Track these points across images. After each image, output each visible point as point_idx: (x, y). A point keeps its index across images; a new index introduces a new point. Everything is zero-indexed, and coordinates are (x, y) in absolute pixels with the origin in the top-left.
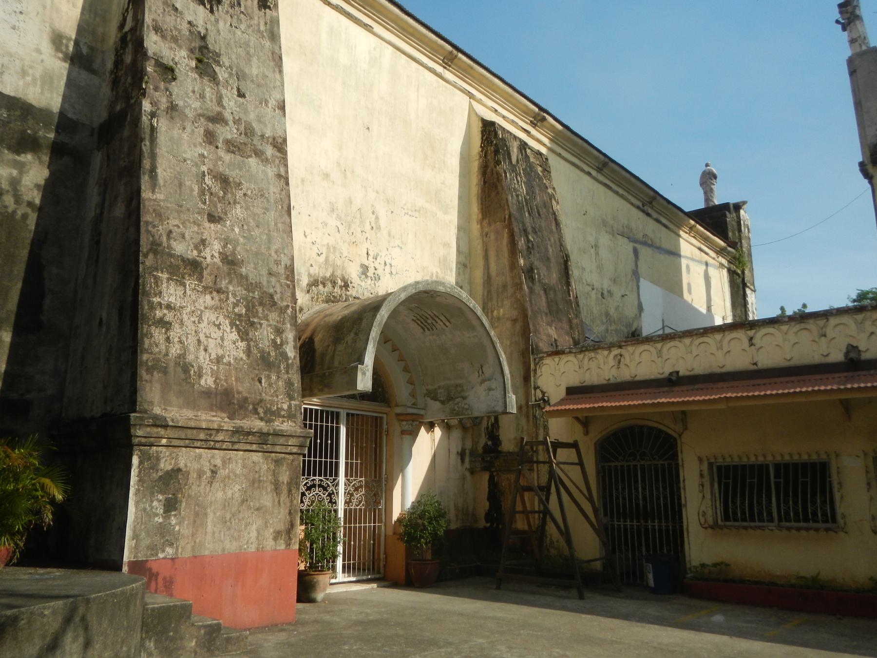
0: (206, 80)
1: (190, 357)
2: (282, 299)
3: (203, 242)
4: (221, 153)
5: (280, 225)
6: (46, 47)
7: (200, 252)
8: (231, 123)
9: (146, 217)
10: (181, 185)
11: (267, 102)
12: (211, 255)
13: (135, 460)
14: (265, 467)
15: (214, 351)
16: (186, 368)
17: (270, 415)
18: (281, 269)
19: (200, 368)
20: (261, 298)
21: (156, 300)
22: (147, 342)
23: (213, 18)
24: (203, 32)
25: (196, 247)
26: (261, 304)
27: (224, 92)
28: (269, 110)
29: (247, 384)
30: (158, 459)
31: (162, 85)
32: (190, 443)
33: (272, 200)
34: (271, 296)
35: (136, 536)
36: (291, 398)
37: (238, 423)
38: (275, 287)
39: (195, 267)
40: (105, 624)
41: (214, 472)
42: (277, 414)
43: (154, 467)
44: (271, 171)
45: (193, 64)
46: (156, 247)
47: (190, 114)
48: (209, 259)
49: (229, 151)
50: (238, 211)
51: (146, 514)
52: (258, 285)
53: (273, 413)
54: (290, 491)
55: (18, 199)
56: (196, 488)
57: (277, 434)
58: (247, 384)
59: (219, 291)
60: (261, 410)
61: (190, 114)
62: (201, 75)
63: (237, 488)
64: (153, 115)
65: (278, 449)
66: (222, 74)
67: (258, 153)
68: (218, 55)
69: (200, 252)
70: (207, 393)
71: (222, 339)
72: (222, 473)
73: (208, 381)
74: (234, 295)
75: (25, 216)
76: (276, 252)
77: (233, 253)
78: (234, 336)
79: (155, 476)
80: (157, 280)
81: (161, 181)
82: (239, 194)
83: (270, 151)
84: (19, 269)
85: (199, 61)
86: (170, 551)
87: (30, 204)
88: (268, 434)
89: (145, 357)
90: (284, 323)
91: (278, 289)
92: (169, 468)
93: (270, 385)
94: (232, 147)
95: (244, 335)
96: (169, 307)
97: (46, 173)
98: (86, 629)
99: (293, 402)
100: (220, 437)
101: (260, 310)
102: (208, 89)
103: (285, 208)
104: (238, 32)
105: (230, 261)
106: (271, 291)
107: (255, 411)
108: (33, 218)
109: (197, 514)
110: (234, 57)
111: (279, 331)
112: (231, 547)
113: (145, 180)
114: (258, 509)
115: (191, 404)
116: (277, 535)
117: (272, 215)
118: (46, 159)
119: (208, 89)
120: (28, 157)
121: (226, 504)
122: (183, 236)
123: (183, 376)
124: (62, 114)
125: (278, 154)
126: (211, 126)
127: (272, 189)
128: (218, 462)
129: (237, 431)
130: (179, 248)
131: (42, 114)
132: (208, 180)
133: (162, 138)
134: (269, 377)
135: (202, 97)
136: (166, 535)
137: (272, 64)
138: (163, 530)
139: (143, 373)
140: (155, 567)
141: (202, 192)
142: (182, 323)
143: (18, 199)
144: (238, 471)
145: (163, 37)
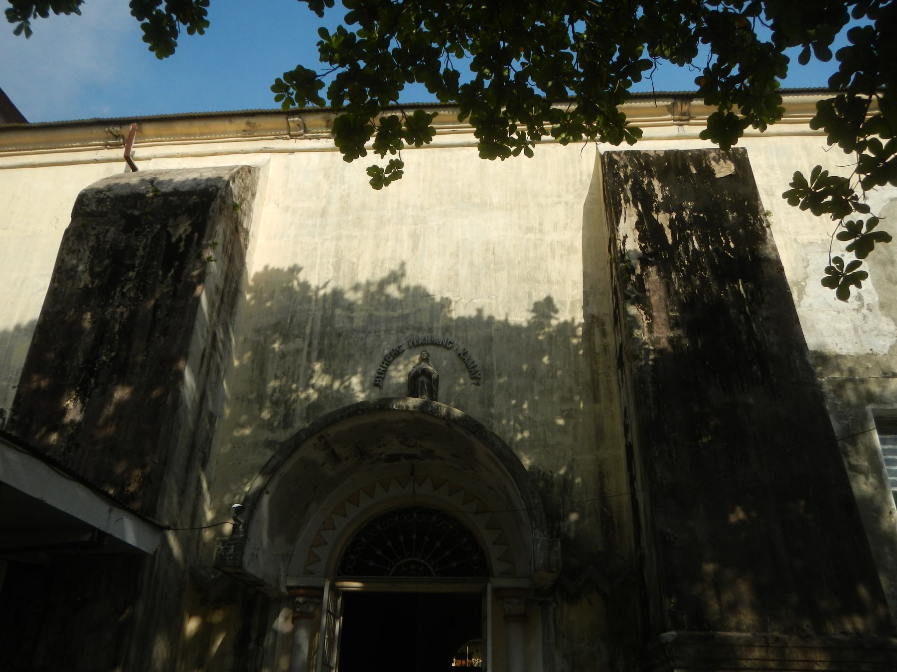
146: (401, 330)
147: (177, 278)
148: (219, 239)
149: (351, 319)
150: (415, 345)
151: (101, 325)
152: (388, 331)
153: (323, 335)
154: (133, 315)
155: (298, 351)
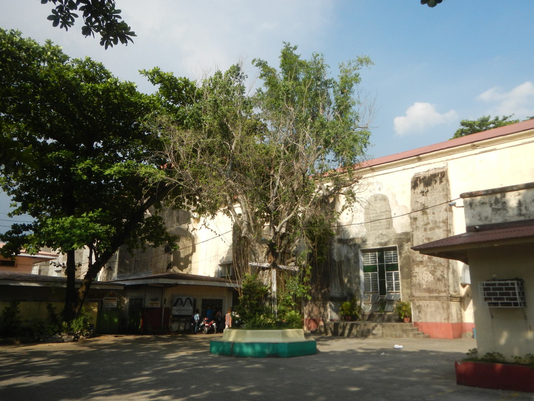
0: (424, 216)
1: (421, 282)
11: (441, 211)
16: (420, 285)
17: (440, 292)
20: (438, 264)
21: (413, 272)
23: (426, 197)
24: (423, 203)
26: (438, 266)
28: (441, 213)
32: (421, 300)
34: (441, 263)
35: (414, 317)
37: (431, 295)
41: (427, 305)
42: (441, 292)
43: (415, 304)
44: (441, 230)
49: (430, 230)
53: (440, 291)
54: (447, 309)
59: (427, 266)
60: (437, 291)
61: (421, 226)
62: (423, 215)
67: (438, 227)
70: (424, 289)
72: (429, 305)
73: (424, 287)
78: (431, 275)
79: (416, 306)
80: (414, 267)
83: (441, 225)
86: (420, 321)
94: (432, 229)
95: (433, 275)
96: (416, 273)
101: (437, 268)
104: (433, 196)
107: (436, 292)
111: (442, 272)
112: (434, 321)
116: (445, 319)
121: (431, 312)
125: (444, 224)
128: (428, 303)
129: (430, 297)
133: (415, 236)
135: (424, 220)
138: (419, 317)
140: (418, 323)
142: (419, 275)
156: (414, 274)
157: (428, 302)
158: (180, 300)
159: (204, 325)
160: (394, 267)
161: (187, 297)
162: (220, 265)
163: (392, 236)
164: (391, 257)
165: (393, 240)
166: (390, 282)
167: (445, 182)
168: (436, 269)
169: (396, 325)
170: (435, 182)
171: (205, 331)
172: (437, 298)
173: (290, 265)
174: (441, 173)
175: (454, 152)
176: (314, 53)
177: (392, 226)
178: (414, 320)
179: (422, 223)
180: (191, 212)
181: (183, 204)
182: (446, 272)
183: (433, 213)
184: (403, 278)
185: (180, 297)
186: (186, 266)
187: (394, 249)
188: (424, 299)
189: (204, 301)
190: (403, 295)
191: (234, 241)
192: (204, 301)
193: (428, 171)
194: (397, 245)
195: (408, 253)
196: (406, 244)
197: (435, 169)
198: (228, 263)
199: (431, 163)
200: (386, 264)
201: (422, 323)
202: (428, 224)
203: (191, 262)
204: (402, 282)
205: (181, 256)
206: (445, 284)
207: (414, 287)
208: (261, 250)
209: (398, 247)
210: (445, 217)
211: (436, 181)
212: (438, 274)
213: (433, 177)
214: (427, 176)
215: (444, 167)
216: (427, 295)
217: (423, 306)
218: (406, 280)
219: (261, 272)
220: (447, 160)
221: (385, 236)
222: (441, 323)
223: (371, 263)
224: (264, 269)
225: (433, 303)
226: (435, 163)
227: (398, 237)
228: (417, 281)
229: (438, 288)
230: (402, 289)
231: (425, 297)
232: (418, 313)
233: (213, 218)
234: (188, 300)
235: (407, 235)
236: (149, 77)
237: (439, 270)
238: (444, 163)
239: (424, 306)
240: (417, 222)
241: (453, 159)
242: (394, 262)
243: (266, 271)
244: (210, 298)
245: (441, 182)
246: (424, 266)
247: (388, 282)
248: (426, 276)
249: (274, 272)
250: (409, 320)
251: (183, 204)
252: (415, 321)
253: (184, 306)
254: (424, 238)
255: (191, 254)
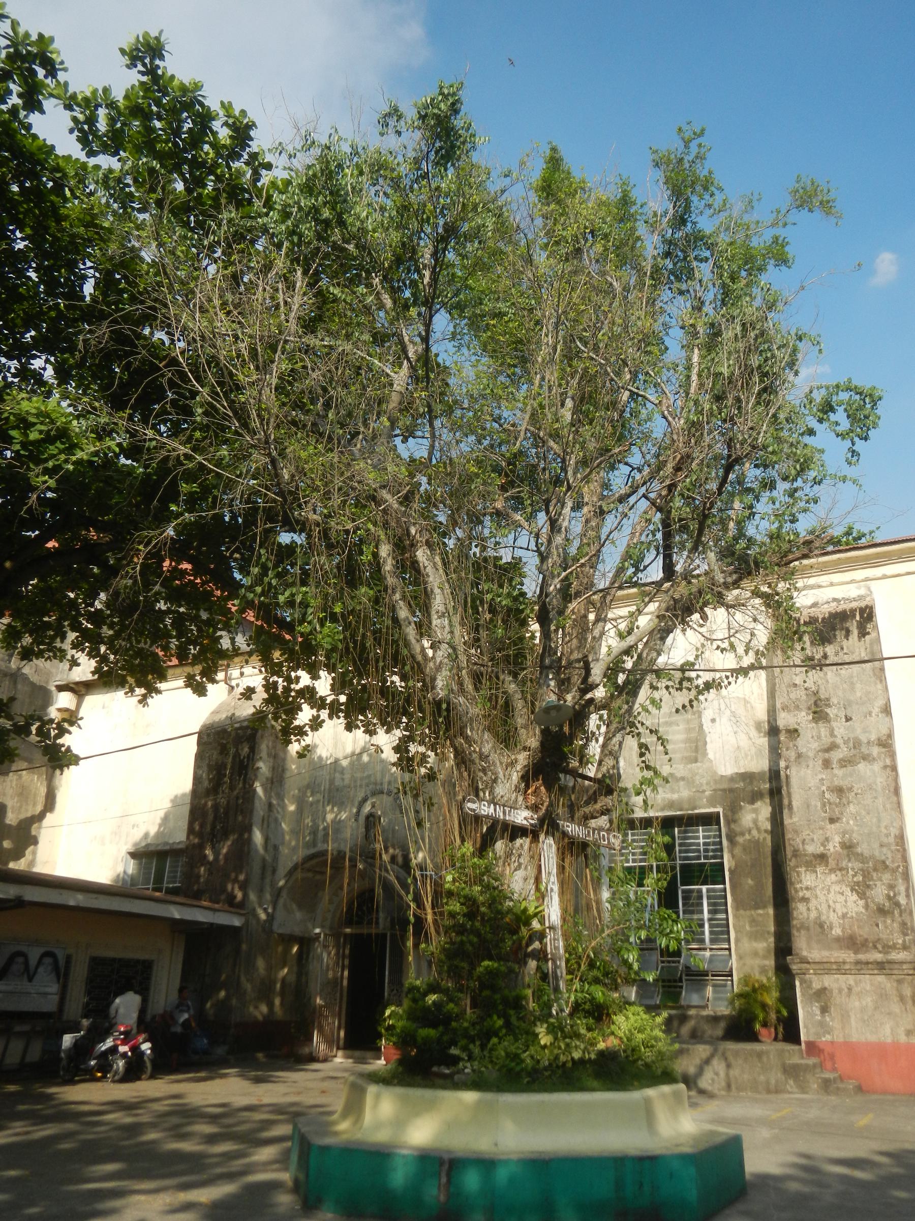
0: (821, 724)
1: (824, 918)
2: (893, 862)
3: (827, 839)
4: (836, 771)
5: (888, 806)
6: (753, 733)
7: (825, 846)
8: (842, 745)
9: (788, 836)
10: (808, 806)
11: (870, 713)
12: (834, 847)
13: (797, 983)
14: (889, 985)
15: (840, 910)
16: (821, 926)
17: (888, 948)
18: (891, 839)
19: (831, 923)
21: (798, 886)
22: (795, 913)
25: (823, 845)
26: (875, 870)
27: (834, 724)
28: (873, 719)
29: (867, 929)
30: (811, 982)
31: (791, 745)
32: (828, 972)
33: (879, 789)
34: (884, 862)
35: (806, 1026)
36: (905, 934)
37: (862, 957)
38: (887, 855)
39: (822, 858)
40: (740, 1062)
41: (850, 989)
42: (894, 947)
43: (810, 987)
44: (877, 767)
45: (811, 717)
46: (796, 853)
47: (811, 754)
48: (832, 850)
49: (842, 766)
50: (852, 808)
51: (810, 1015)
52: (872, 857)
53: (889, 947)
55: (758, 829)
56: (838, 999)
57: (890, 962)
58: (867, 929)
59: (841, 870)
60: (879, 947)
61: (811, 754)
62: (816, 723)
63: (869, 999)
64: (787, 767)
65: (896, 972)
66: (832, 712)
67: (866, 758)
68: (828, 700)
69: (825, 846)
70: (838, 939)
71: (846, 901)
72: (856, 990)
73: (837, 931)
74: (853, 869)
75: (765, 839)
76: (886, 827)
77: (850, 840)
78: (855, 897)
79: (811, 992)
80: (798, 873)
81: (795, 809)
82: (851, 796)
83: (875, 751)
84: (769, 870)
85: (815, 713)
86: (828, 1038)
87: (766, 831)
88: (882, 963)
89: (795, 922)
90: (896, 879)
91: (889, 855)
92: (819, 987)
93: (886, 927)
94: (845, 763)
95: (862, 895)
96: (807, 888)
97: (770, 809)
98: (726, 1059)
99: (907, 938)
100: (847, 967)
101: (875, 875)
102: (823, 730)
103: (892, 789)
105: (848, 847)
106: (883, 858)
107: (875, 947)
108: (769, 838)
109: (842, 1016)
110: (840, 693)
111: (891, 887)
112: (872, 1038)
113: (786, 811)
114: (889, 1014)
115: (830, 948)
117: (880, 800)
118: (768, 801)
119: (823, 730)
120: (759, 804)
121: (863, 1010)
122: (813, 840)
123: (819, 930)
124: (770, 770)
126: (827, 755)
127: (879, 780)
128: (852, 983)
129: (858, 963)
130: (811, 849)
131: (761, 774)
132: (827, 795)
133: (794, 781)
134: (885, 922)
135: (819, 737)
136: (824, 1027)
137: (873, 679)
138: (822, 1024)
139: (795, 932)
140: (821, 1046)
141: (824, 805)
142: (816, 897)
143: (758, 829)
144: (868, 988)
145: (789, 711)
146: (367, 785)
147: (245, 782)
148: (264, 754)
149: (343, 779)
150: (374, 794)
151: (216, 807)
152: (361, 786)
153: (330, 791)
154: (228, 802)
155: (318, 801)
156: (801, 894)
157: (851, 979)
158: (20, 960)
159: (114, 1050)
160: (715, 874)
161: (42, 950)
162: (133, 855)
163: (704, 781)
164: (698, 844)
165: (707, 793)
166: (695, 917)
167: (873, 635)
168: (872, 879)
169: (767, 1053)
170: (844, 632)
171: (116, 1072)
172: (882, 967)
173: (593, 823)
174: (862, 610)
175: (889, 559)
176: (685, 127)
177: (705, 754)
178: (808, 1032)
179: (815, 745)
180: (53, 689)
181: (58, 644)
182: (902, 888)
183: (848, 719)
184: (738, 905)
185: (24, 949)
186: (18, 854)
187: (709, 820)
188: (839, 968)
189: (96, 963)
190: (740, 957)
191: (197, 779)
192: (96, 963)
193: (815, 605)
194: (720, 809)
195: (755, 833)
196: (749, 807)
197: (835, 600)
198: (159, 848)
199: (820, 587)
200: (682, 866)
201: (832, 1043)
202: (833, 747)
203: (35, 841)
204: (735, 916)
205: (8, 821)
206: (904, 924)
207: (803, 932)
208: (505, 760)
209: (725, 816)
210: (885, 731)
211: (848, 633)
212: (879, 893)
213: (837, 621)
214: (821, 617)
215: (861, 598)
216: (849, 956)
217: (835, 992)
218: (748, 913)
219: (500, 846)
220: (867, 579)
221: (682, 783)
222: (896, 1045)
223: (634, 861)
224: (516, 832)
225: (868, 982)
226: (832, 584)
227: (725, 786)
228: (813, 915)
229: (883, 936)
230: (737, 940)
231: (844, 963)
232: (818, 1012)
233: (143, 701)
234: (48, 960)
235: (751, 783)
236: (75, 119)
237: (878, 883)
238: (859, 588)
239: (840, 991)
240: (800, 742)
241: (885, 577)
242: (706, 857)
243: (519, 841)
244: (117, 956)
245: (863, 634)
246: (832, 871)
247: (688, 916)
248: (841, 899)
249: (549, 847)
250: (773, 1035)
251: (58, 644)
252: (811, 1039)
253: (30, 980)
254: (824, 788)
255: (41, 817)
